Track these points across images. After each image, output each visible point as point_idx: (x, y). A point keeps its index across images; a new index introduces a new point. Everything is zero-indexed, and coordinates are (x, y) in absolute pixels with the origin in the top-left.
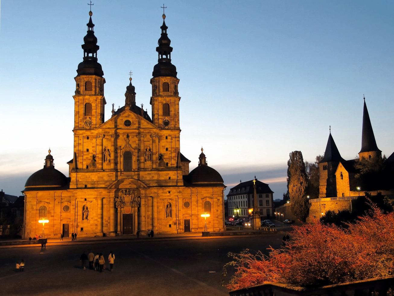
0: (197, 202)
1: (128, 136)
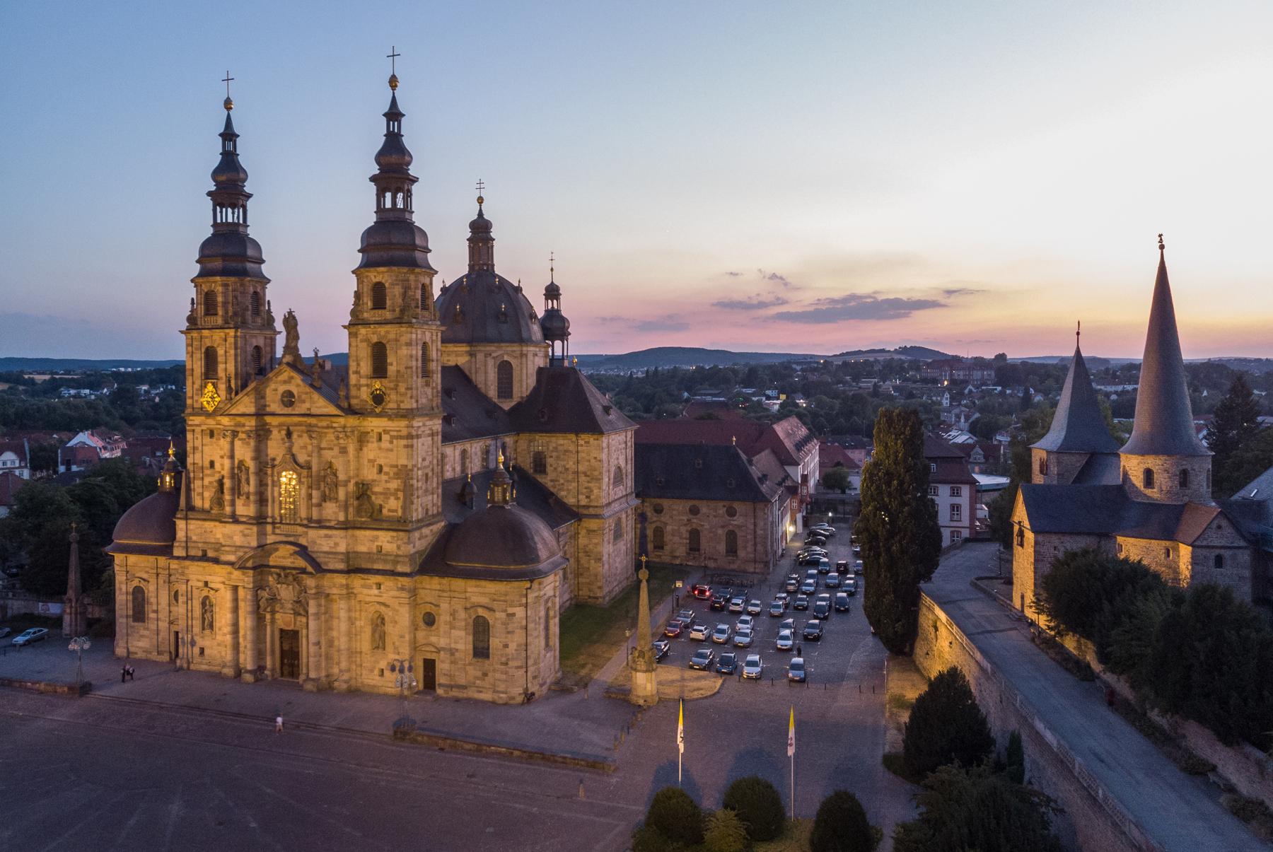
0: (453, 614)
1: (289, 434)
